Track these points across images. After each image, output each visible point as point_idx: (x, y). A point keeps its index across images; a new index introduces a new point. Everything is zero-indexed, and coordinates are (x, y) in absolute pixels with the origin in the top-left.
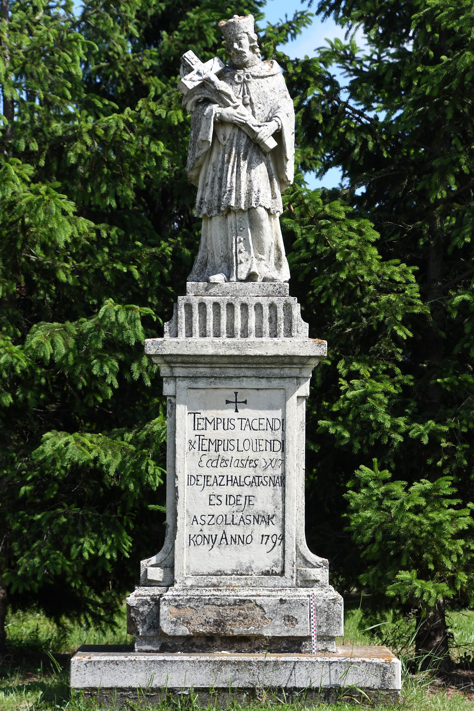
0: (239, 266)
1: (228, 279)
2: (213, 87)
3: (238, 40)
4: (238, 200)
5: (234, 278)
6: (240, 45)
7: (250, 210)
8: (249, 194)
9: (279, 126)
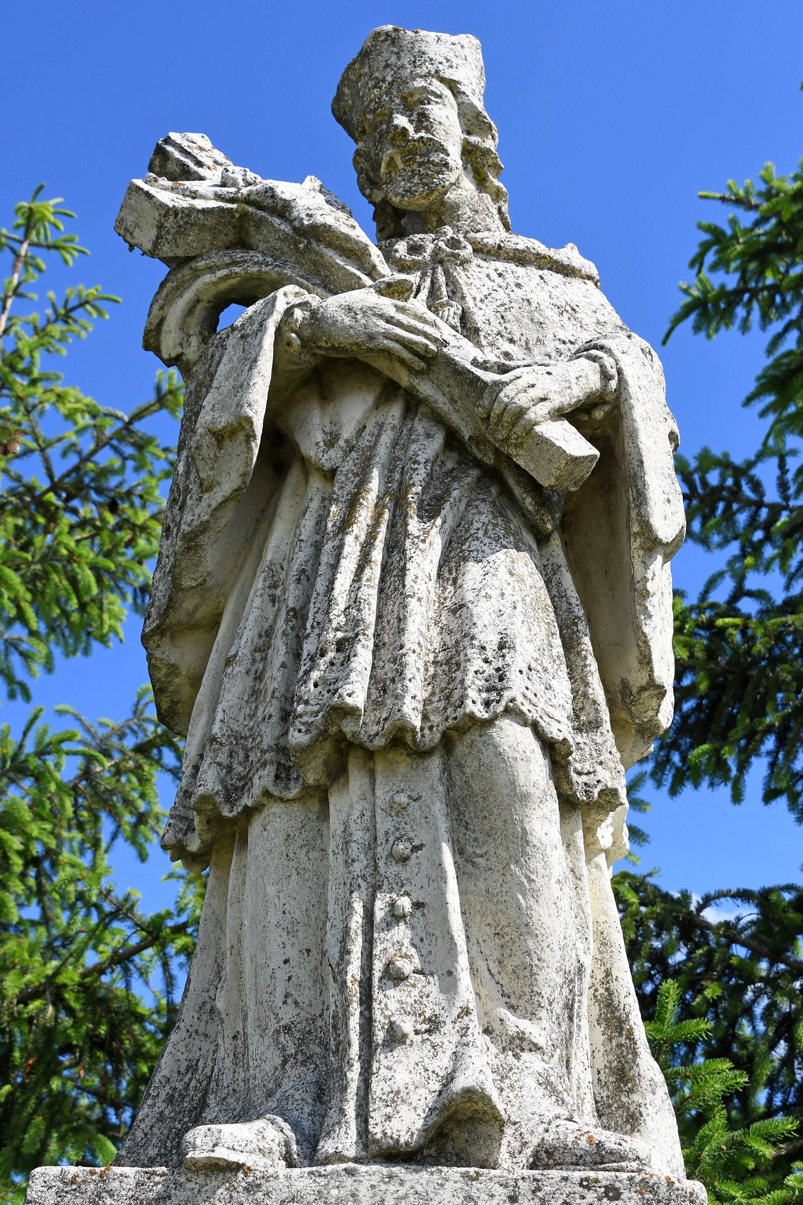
0: (382, 1060)
1: (308, 1149)
2: (285, 227)
3: (416, 106)
4: (385, 685)
5: (345, 1140)
6: (422, 121)
7: (457, 738)
8: (450, 663)
9: (605, 376)
